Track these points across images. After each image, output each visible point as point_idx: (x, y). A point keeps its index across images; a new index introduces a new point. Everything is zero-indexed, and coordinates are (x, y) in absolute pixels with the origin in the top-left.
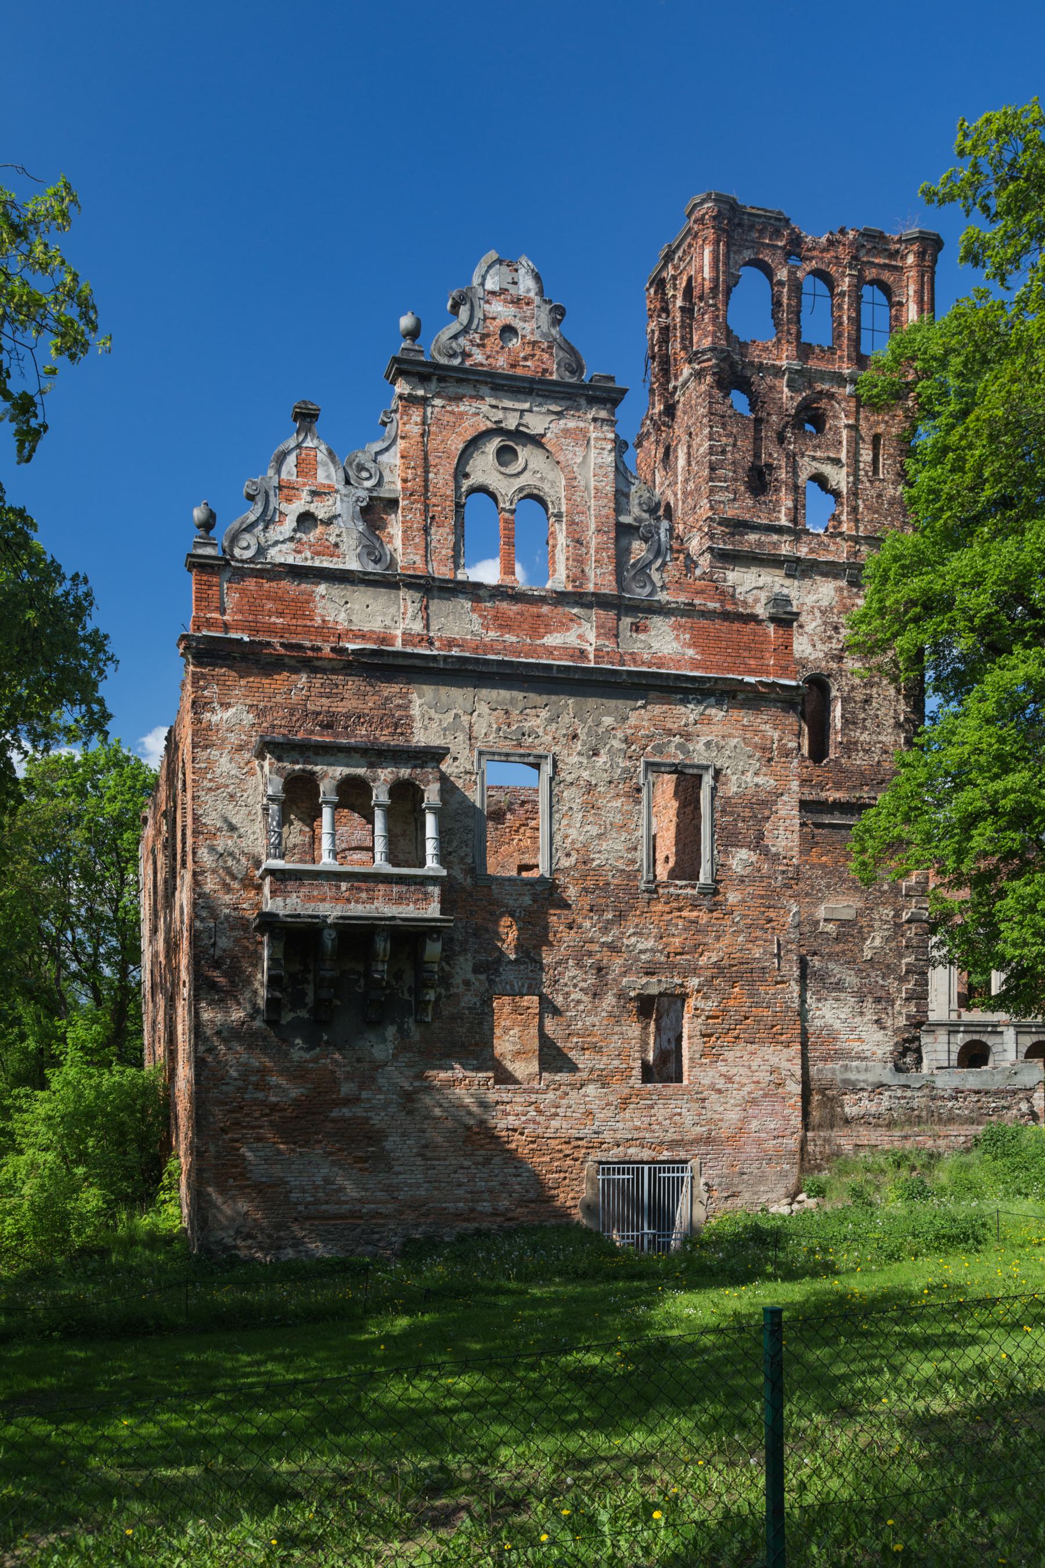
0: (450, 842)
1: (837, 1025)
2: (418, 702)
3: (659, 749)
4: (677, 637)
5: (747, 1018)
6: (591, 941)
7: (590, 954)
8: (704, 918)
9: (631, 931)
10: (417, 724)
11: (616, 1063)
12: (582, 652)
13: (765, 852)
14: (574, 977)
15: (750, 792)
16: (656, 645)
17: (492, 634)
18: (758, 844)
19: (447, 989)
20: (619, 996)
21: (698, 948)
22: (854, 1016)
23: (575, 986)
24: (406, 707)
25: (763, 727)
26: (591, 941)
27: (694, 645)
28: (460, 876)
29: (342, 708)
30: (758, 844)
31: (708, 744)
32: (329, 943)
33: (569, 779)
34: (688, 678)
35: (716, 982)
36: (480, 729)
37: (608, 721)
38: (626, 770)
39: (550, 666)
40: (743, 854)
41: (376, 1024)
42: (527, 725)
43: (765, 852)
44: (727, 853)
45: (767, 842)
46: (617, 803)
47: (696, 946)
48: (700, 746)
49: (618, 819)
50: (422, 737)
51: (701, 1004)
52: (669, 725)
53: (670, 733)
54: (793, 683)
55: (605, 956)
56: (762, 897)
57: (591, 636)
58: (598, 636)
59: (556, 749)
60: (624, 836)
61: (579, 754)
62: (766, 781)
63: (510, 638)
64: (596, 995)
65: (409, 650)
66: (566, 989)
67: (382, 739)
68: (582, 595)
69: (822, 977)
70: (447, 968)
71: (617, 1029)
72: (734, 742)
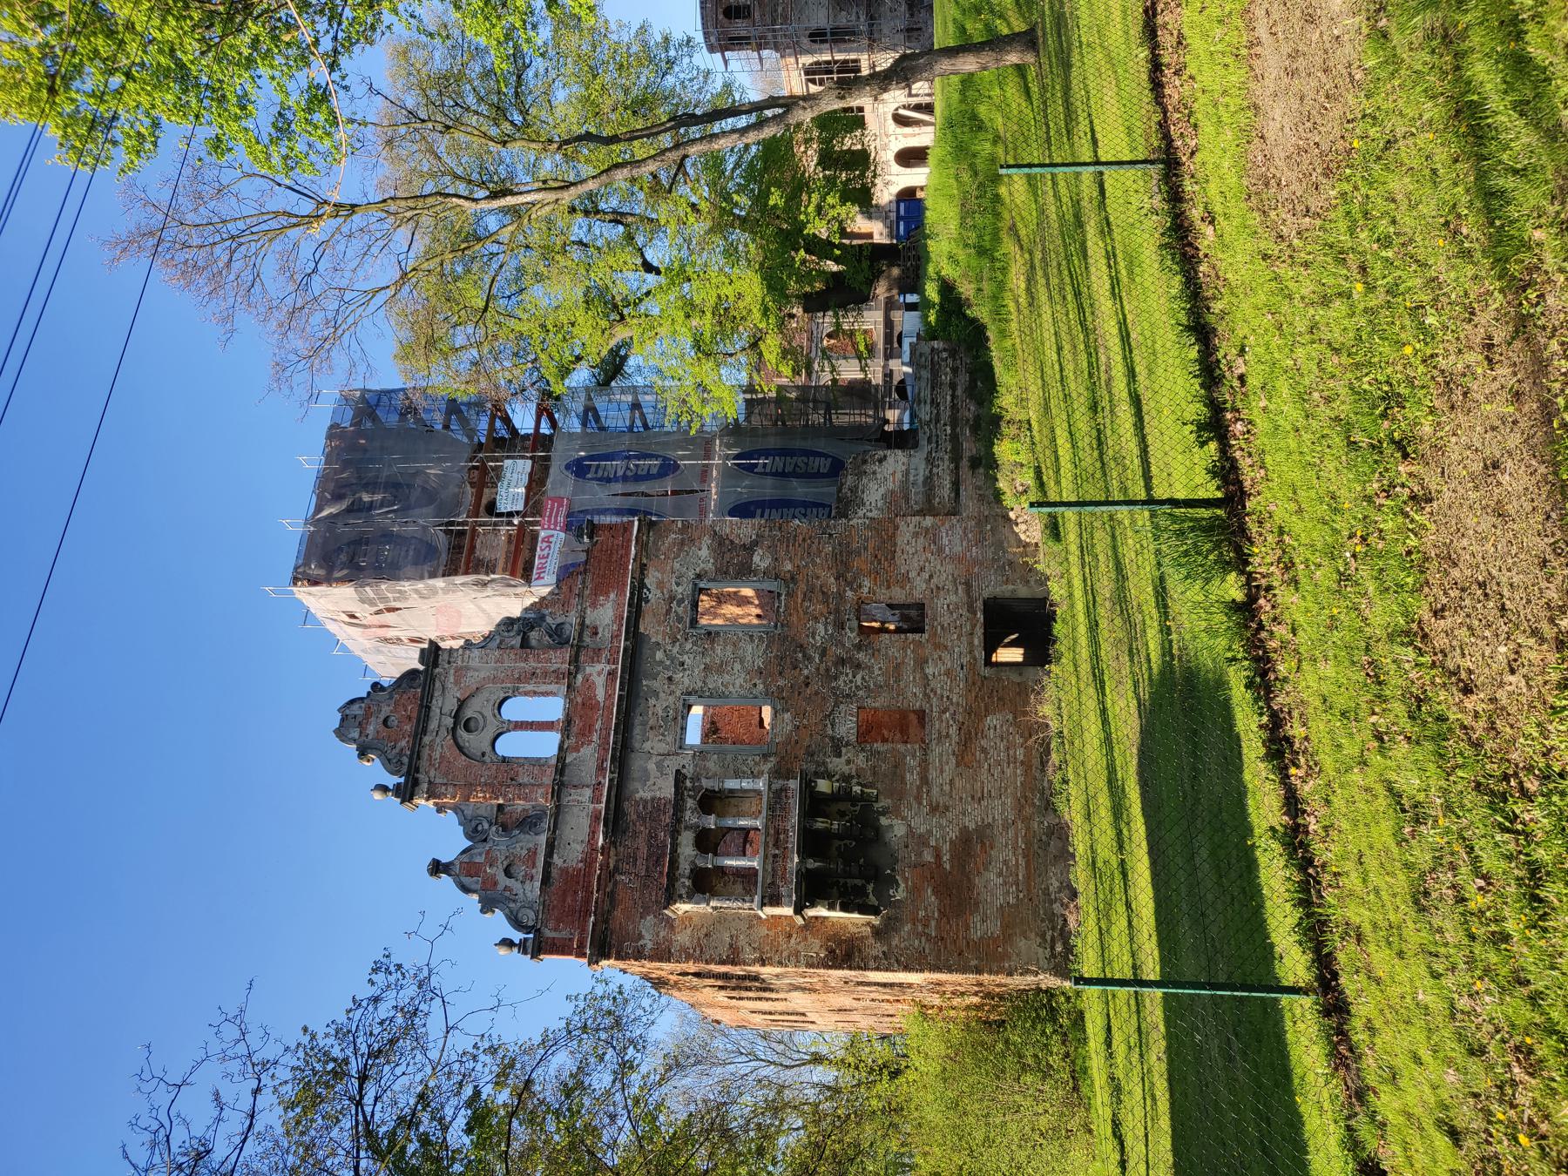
0: (744, 772)
2: (641, 793)
3: (680, 619)
4: (602, 605)
6: (818, 669)
7: (827, 670)
8: (803, 586)
10: (658, 794)
11: (909, 652)
12: (609, 674)
13: (755, 543)
16: (607, 621)
17: (595, 738)
18: (750, 548)
19: (853, 777)
20: (859, 647)
23: (851, 682)
24: (646, 802)
26: (818, 669)
27: (607, 594)
28: (769, 765)
29: (644, 851)
30: (750, 548)
31: (678, 584)
32: (817, 864)
33: (700, 684)
34: (631, 598)
35: (849, 579)
36: (662, 747)
37: (659, 655)
38: (694, 644)
39: (620, 696)
40: (756, 558)
41: (878, 831)
42: (660, 713)
43: (755, 543)
44: (756, 570)
46: (718, 649)
47: (823, 593)
48: (680, 589)
49: (729, 648)
50: (667, 790)
51: (866, 590)
53: (668, 611)
54: (636, 523)
55: (830, 659)
57: (599, 667)
58: (599, 662)
59: (678, 693)
62: (706, 540)
63: (598, 726)
64: (858, 666)
65: (604, 799)
67: (668, 820)
68: (570, 673)
70: (837, 777)
72: (677, 566)
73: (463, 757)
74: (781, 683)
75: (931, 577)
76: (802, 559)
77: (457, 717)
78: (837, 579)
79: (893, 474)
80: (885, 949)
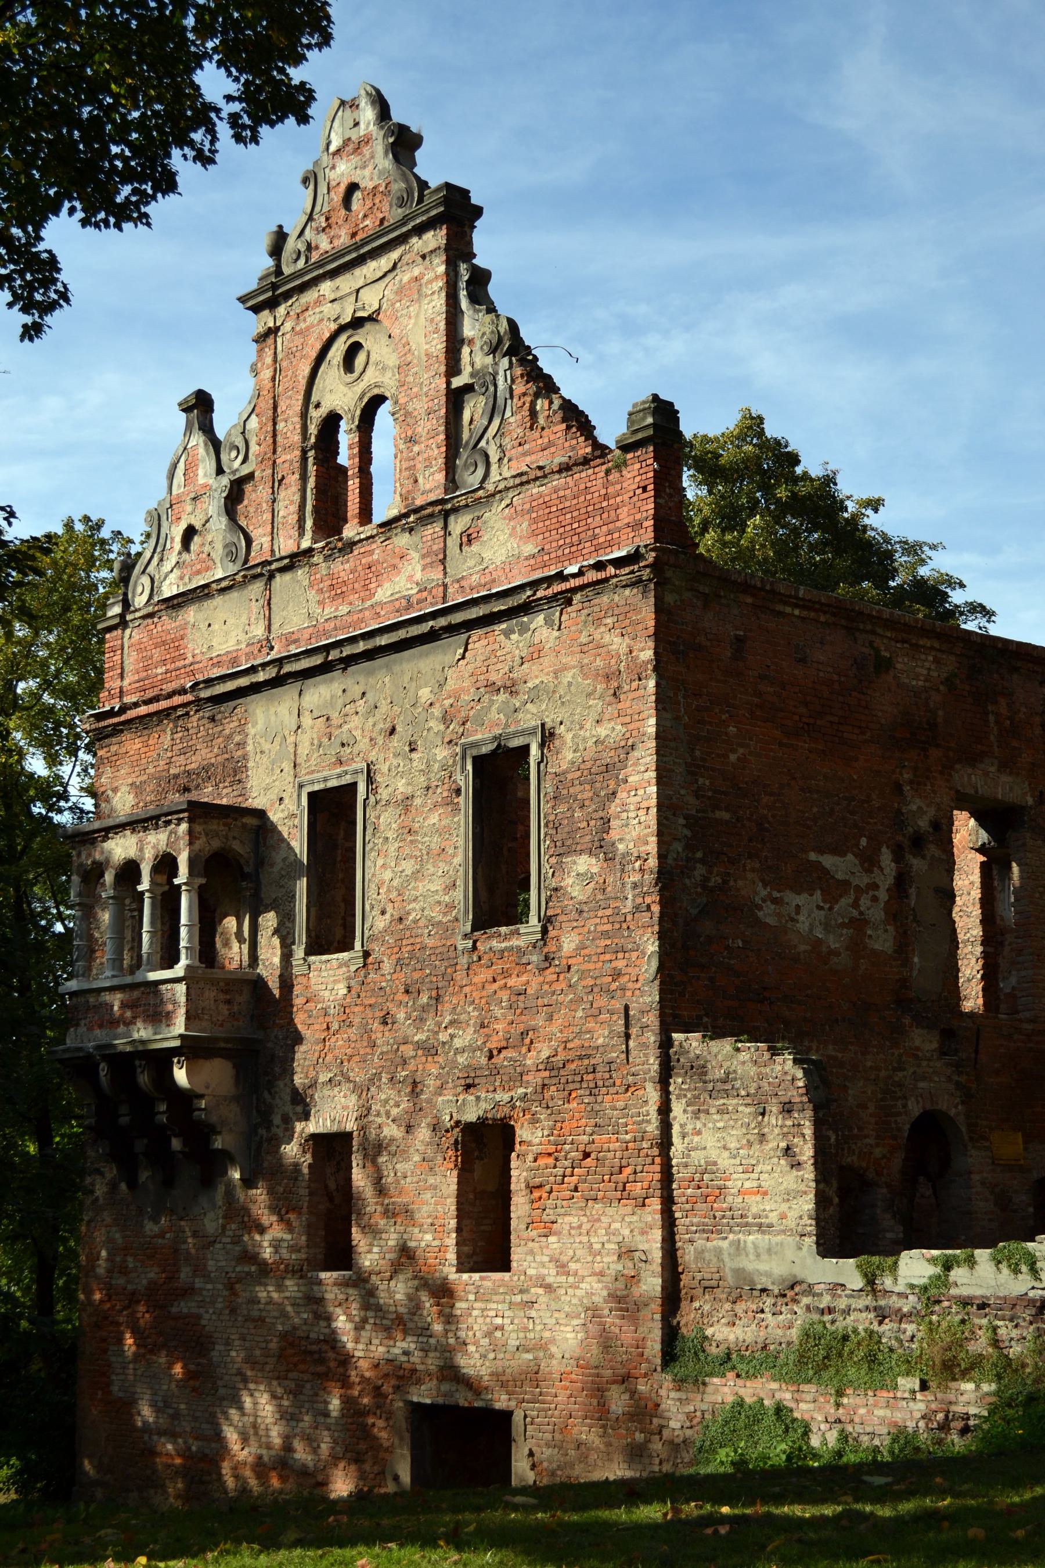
1: (724, 1161)
5: (587, 1155)
9: (448, 1019)
14: (386, 1101)
15: (589, 754)
21: (525, 1038)
22: (750, 1144)
25: (607, 638)
40: (584, 863)
45: (614, 835)
46: (434, 819)
49: (435, 842)
52: (493, 677)
53: (493, 688)
56: (605, 934)
59: (372, 756)
60: (443, 866)
61: (397, 755)
62: (611, 731)
64: (409, 1129)
66: (379, 1120)
69: (698, 1070)
71: (431, 1181)
72: (567, 677)
73: (305, 370)
74: (387, 967)
75: (548, 1288)
76: (583, 974)
77: (357, 323)
78: (548, 1065)
79: (761, 1192)
80: (101, 1201)
